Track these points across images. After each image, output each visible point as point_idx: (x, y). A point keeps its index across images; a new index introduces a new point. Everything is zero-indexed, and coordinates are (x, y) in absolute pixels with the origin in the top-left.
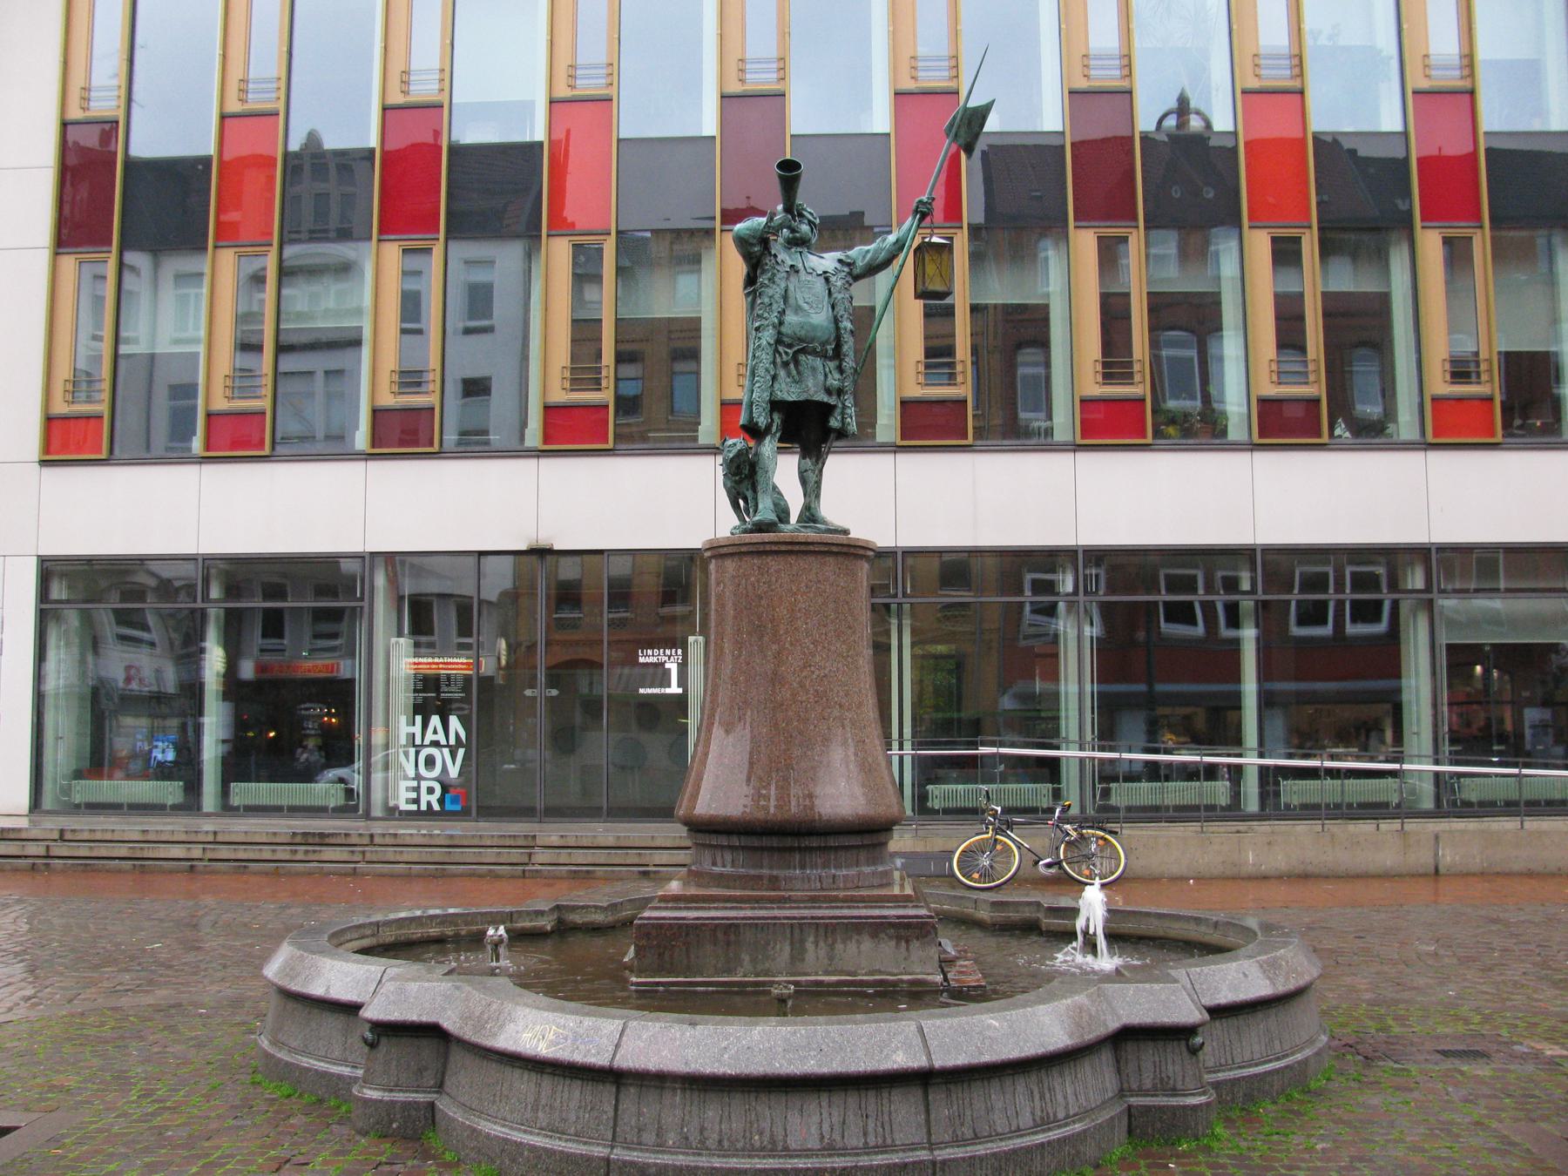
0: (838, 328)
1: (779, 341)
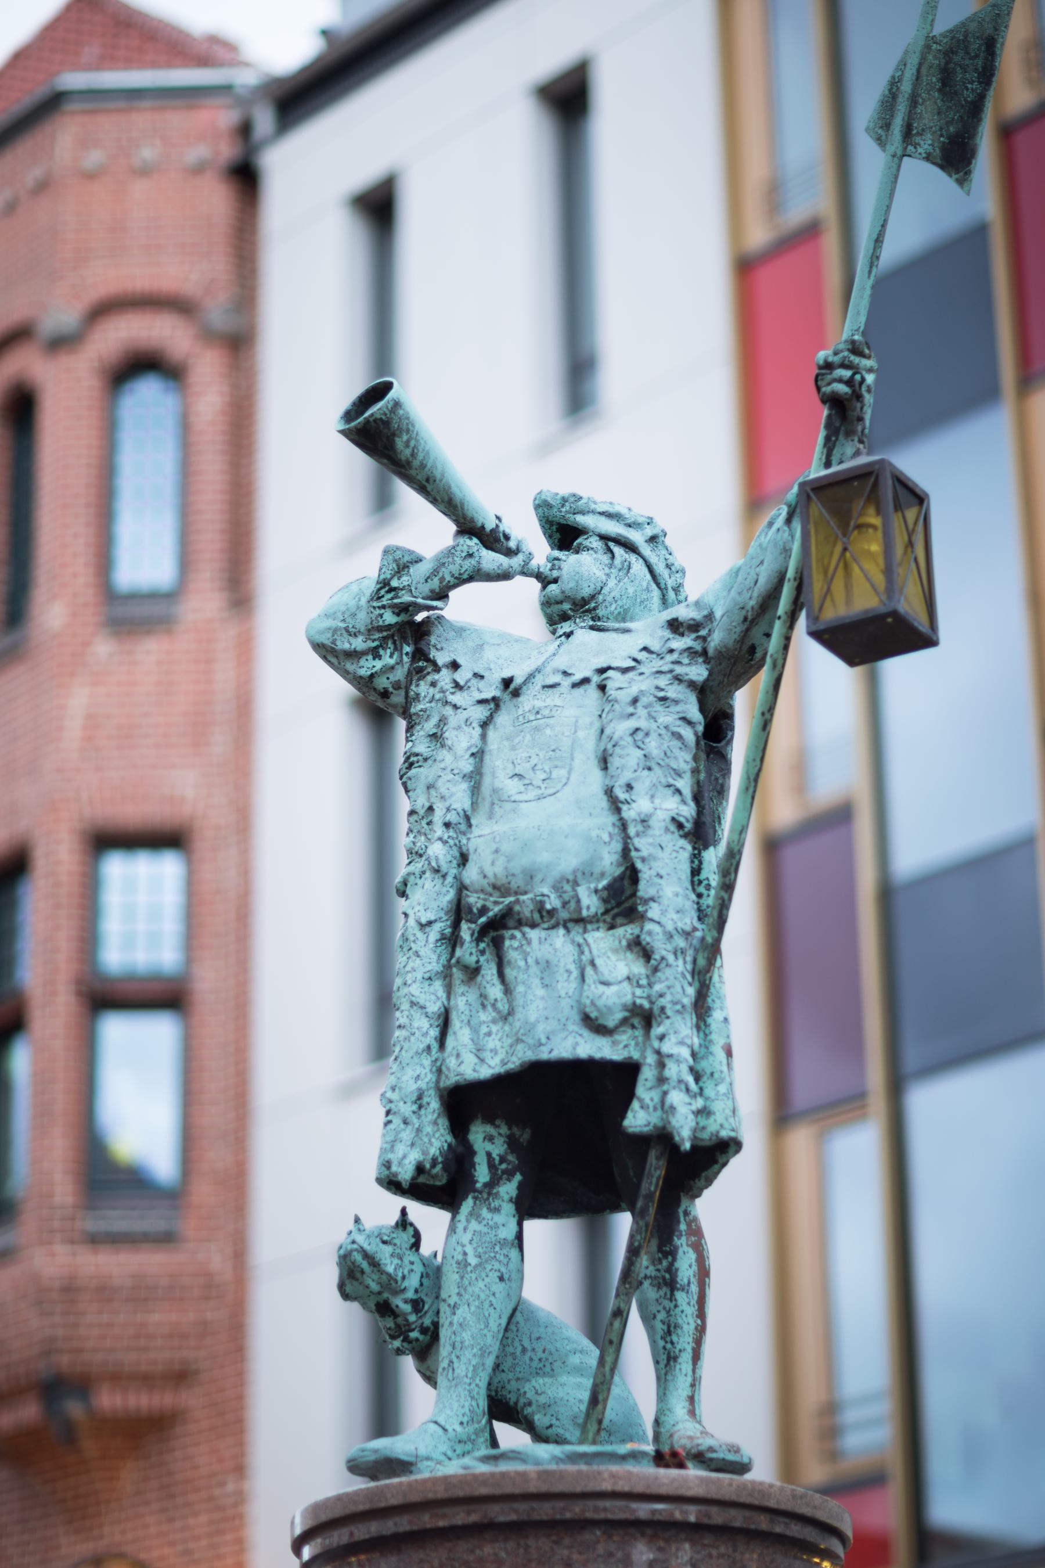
0: (624, 826)
1: (459, 912)
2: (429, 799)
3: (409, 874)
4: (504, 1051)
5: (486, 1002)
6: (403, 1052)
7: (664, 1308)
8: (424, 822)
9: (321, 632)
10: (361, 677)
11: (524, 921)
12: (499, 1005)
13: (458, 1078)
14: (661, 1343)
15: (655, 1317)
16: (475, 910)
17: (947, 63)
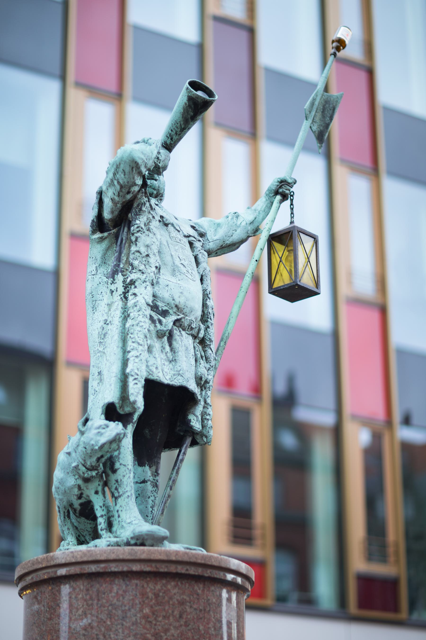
2: (147, 251)
3: (139, 278)
4: (170, 375)
5: (163, 351)
6: (142, 356)
7: (154, 496)
8: (144, 259)
9: (139, 158)
10: (135, 183)
11: (182, 326)
12: (168, 354)
13: (158, 378)
14: (151, 509)
15: (149, 498)
16: (160, 309)
17: (325, 105)
